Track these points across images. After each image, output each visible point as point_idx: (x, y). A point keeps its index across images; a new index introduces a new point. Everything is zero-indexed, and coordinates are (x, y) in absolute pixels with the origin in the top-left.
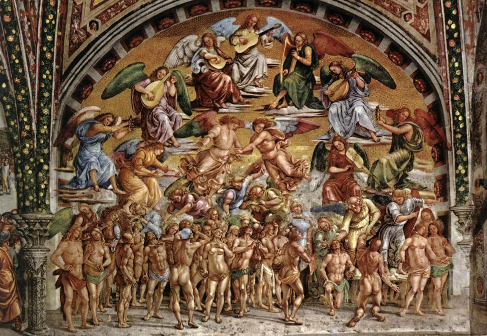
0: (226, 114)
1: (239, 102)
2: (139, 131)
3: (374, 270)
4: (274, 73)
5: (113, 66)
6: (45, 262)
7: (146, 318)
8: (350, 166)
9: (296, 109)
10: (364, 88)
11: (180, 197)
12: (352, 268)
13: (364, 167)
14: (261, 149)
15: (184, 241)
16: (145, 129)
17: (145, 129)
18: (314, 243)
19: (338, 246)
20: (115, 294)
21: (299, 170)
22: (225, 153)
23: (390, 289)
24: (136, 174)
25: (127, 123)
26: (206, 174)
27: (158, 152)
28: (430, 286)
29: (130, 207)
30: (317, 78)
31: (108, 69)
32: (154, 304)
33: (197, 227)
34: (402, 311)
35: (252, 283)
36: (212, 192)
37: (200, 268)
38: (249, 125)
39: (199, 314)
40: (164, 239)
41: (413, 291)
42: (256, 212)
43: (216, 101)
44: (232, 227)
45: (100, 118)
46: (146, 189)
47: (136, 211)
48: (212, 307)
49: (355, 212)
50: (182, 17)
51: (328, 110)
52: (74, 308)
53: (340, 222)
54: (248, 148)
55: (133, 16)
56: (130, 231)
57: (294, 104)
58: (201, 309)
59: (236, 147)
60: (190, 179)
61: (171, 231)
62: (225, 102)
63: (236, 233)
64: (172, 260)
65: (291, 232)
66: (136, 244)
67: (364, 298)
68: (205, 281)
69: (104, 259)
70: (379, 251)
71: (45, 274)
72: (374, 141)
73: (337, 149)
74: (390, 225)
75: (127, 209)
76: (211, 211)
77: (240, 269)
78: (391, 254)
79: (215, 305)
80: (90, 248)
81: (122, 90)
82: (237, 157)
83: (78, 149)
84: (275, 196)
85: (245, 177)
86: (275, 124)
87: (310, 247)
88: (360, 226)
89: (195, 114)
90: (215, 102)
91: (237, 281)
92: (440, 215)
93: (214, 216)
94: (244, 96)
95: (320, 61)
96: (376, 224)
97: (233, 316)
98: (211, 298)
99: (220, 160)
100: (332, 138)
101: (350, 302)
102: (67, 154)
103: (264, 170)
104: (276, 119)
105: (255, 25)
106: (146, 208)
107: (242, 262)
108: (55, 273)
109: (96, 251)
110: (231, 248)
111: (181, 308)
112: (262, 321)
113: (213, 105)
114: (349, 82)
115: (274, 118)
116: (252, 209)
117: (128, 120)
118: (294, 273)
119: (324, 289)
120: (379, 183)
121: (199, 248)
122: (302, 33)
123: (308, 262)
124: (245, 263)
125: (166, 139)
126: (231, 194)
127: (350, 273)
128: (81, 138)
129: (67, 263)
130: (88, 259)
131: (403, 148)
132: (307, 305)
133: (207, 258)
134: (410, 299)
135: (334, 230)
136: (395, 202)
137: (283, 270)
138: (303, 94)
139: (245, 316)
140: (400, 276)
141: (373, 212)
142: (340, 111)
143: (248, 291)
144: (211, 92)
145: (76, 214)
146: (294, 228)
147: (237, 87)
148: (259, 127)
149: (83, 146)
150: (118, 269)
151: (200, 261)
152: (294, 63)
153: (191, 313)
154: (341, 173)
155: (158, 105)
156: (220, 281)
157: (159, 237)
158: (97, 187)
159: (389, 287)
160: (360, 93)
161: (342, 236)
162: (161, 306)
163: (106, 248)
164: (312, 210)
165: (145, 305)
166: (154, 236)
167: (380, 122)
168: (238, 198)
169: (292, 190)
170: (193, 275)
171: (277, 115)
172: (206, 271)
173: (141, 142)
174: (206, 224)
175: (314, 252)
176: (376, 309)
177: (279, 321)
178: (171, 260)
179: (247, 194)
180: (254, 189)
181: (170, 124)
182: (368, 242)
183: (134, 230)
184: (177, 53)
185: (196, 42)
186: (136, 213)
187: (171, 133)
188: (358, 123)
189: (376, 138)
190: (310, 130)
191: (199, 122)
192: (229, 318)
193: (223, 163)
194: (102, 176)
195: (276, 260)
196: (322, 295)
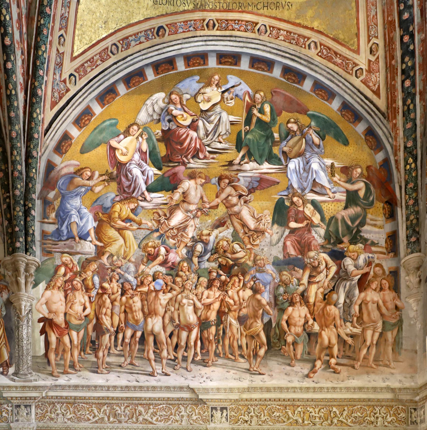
1: (205, 158)
2: (114, 185)
3: (331, 324)
4: (237, 129)
5: (90, 121)
6: (30, 310)
7: (123, 365)
8: (308, 221)
10: (319, 145)
11: (153, 250)
12: (311, 322)
13: (321, 223)
14: (227, 204)
15: (157, 291)
16: (120, 183)
17: (120, 183)
18: (276, 298)
19: (298, 300)
20: (95, 341)
22: (193, 207)
23: (345, 342)
24: (112, 226)
25: (104, 177)
27: (132, 206)
28: (382, 340)
29: (107, 258)
30: (276, 135)
31: (85, 125)
33: (169, 278)
34: (357, 364)
35: (219, 334)
36: (182, 245)
37: (172, 320)
38: (214, 180)
39: (172, 362)
40: (139, 290)
41: (366, 345)
42: (223, 265)
43: (184, 157)
44: (201, 279)
45: (79, 172)
46: (121, 241)
47: (113, 261)
48: (183, 356)
49: (313, 267)
50: (150, 75)
52: (57, 354)
53: (299, 276)
54: (214, 204)
55: (106, 72)
56: (108, 282)
57: (255, 161)
58: (173, 358)
59: (203, 202)
60: (162, 232)
61: (145, 281)
62: (193, 158)
63: (205, 285)
64: (146, 310)
66: (113, 294)
67: (322, 349)
68: (177, 331)
69: (85, 309)
70: (335, 305)
71: (30, 321)
72: (329, 197)
73: (296, 205)
74: (345, 279)
75: (105, 259)
78: (346, 309)
79: (186, 354)
80: (71, 298)
81: (98, 145)
82: (204, 211)
83: (59, 202)
86: (239, 180)
88: (317, 280)
89: (165, 169)
91: (206, 332)
92: (392, 270)
94: (210, 152)
95: (278, 118)
96: (333, 278)
97: (202, 365)
98: (182, 347)
99: (189, 214)
101: (309, 354)
102: (50, 206)
104: (239, 175)
105: (218, 83)
106: (122, 260)
107: (211, 314)
108: (40, 321)
109: (77, 300)
110: (200, 300)
111: (155, 357)
112: (229, 370)
114: (305, 138)
115: (237, 174)
117: (104, 175)
118: (258, 325)
119: (285, 341)
120: (335, 239)
121: (171, 299)
122: (261, 91)
123: (271, 315)
124: (213, 316)
125: (140, 193)
126: (199, 247)
127: (309, 326)
128: (62, 191)
129: (50, 312)
130: (70, 308)
131: (357, 205)
133: (178, 310)
134: (364, 351)
135: (294, 283)
136: (350, 257)
138: (264, 150)
139: (213, 365)
140: (355, 330)
141: (330, 266)
142: (297, 167)
143: (216, 341)
144: (179, 147)
145: (59, 264)
147: (203, 144)
149: (64, 198)
150: (98, 319)
151: (172, 312)
152: (254, 120)
153: (164, 361)
154: (300, 228)
155: (131, 160)
156: (190, 331)
157: (134, 287)
158: (77, 238)
159: (345, 340)
160: (316, 150)
161: (301, 288)
162: (137, 354)
163: (87, 298)
164: (274, 264)
165: (122, 353)
166: (130, 287)
167: (335, 179)
168: (206, 251)
169: (255, 243)
170: (166, 325)
172: (177, 322)
173: (117, 196)
174: (177, 275)
175: (276, 305)
176: (333, 361)
177: (244, 370)
179: (214, 248)
180: (221, 243)
182: (325, 295)
183: (111, 281)
184: (147, 110)
185: (164, 99)
186: (112, 264)
187: (144, 187)
188: (314, 180)
189: (331, 195)
190: (271, 186)
191: (169, 177)
192: (200, 367)
194: (82, 227)
195: (241, 312)
196: (284, 347)
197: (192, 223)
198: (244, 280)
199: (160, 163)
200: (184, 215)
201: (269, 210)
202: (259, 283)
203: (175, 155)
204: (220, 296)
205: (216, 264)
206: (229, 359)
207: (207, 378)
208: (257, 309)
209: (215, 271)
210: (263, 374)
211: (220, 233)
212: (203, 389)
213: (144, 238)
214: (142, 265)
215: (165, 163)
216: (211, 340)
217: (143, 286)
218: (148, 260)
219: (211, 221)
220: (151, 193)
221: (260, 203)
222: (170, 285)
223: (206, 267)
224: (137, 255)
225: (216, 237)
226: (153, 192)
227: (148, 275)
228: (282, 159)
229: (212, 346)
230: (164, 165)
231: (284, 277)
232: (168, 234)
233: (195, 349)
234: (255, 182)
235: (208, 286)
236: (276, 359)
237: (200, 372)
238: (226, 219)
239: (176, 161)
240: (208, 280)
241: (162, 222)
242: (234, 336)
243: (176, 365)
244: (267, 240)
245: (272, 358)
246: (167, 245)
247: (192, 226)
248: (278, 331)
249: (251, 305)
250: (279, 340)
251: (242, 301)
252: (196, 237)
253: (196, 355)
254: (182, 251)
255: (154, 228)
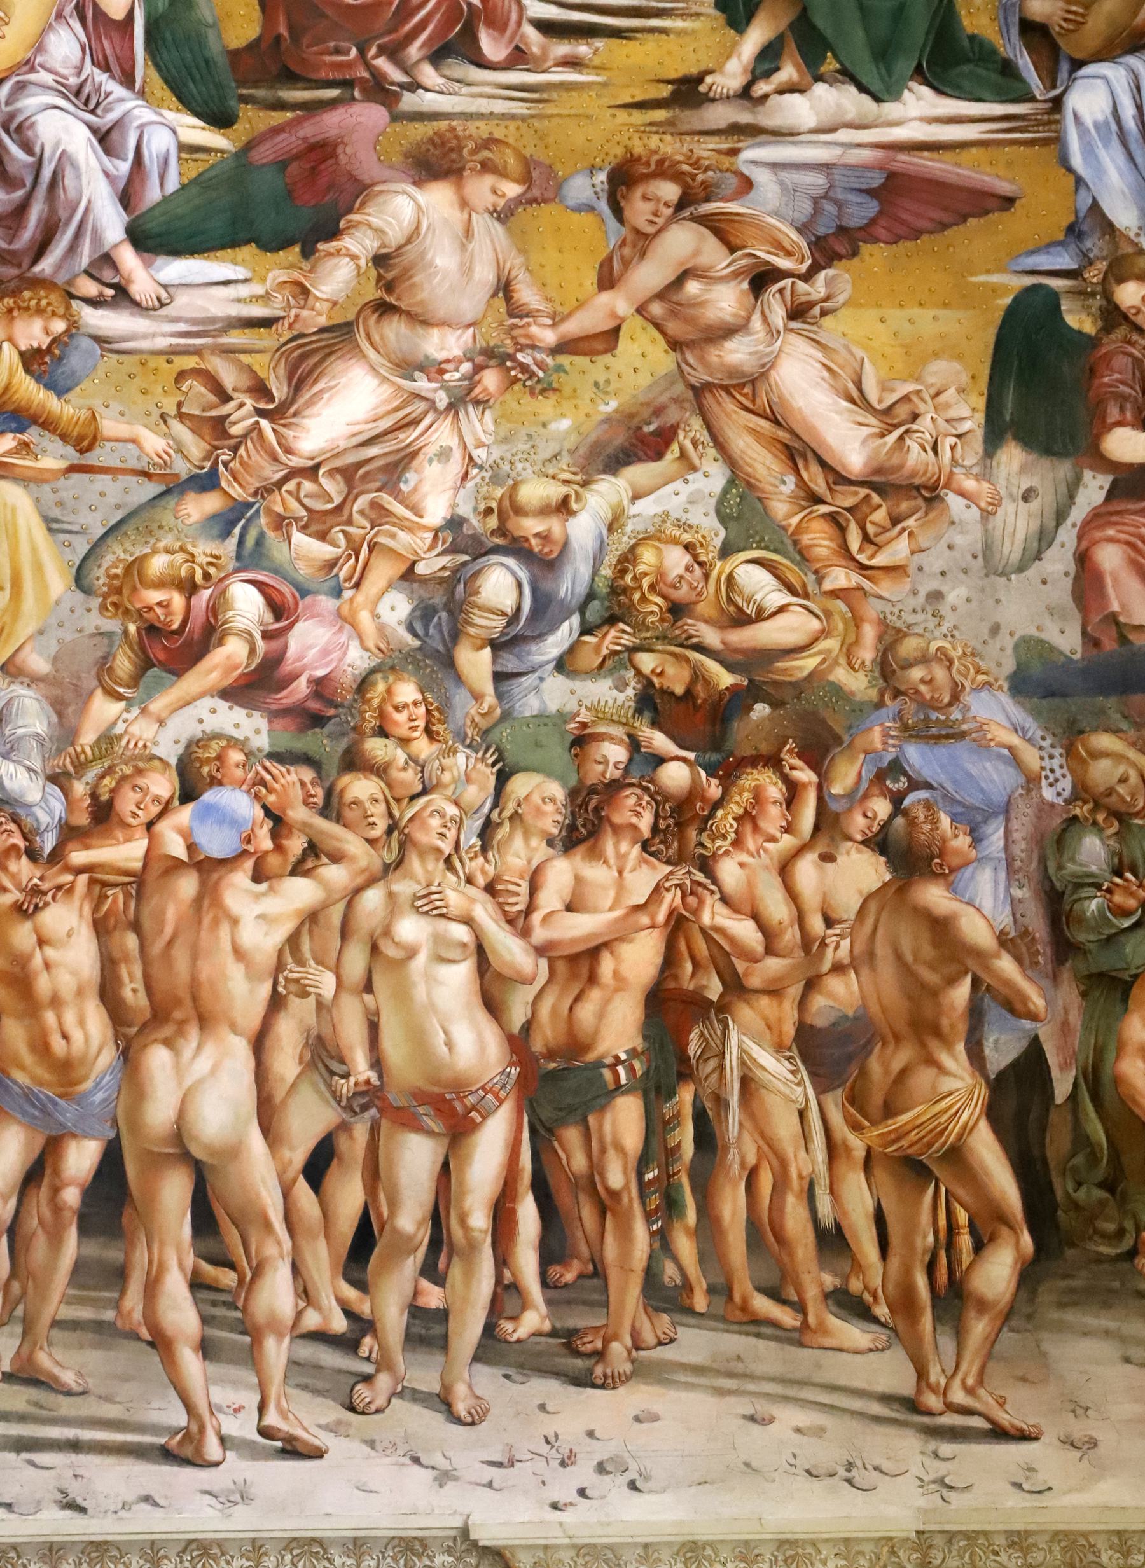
0: (443, 125)
1: (519, 57)
9: (865, 99)
11: (178, 601)
14: (673, 327)
21: (912, 444)
26: (338, 463)
32: (16, 1286)
33: (295, 777)
35: (672, 1153)
36: (383, 572)
39: (331, 1358)
40: (78, 857)
42: (667, 693)
43: (382, 51)
44: (520, 785)
48: (416, 1311)
51: (1057, 104)
57: (848, 75)
58: (339, 1324)
59: (515, 310)
60: (236, 492)
61: (127, 803)
62: (438, 56)
63: (551, 820)
64: (133, 993)
65: (899, 821)
68: (361, 1132)
76: (381, 687)
77: (591, 1057)
79: (433, 1297)
82: (524, 368)
84: (781, 597)
85: (585, 484)
86: (747, 184)
87: (1039, 926)
90: (373, 51)
91: (572, 1135)
93: (401, 717)
94: (547, 28)
97: (557, 1374)
98: (404, 1246)
99: (423, 384)
100: (1103, 265)
103: (695, 443)
104: (748, 154)
107: (601, 1015)
111: (205, 1320)
112: (763, 1408)
113: (364, 74)
115: (734, 152)
116: (638, 673)
118: (947, 1084)
121: (312, 917)
123: (1033, 1017)
125: (85, 257)
132: (1061, 1305)
133: (368, 987)
137: (875, 1065)
139: (642, 1372)
143: (654, 1201)
146: (922, 794)
148: (645, 198)
151: (320, 1005)
155: (29, 65)
157: (48, 843)
162: (66, 1300)
166: (18, 840)
169: (878, 561)
170: (279, 1095)
171: (753, 131)
172: (362, 1069)
174: (353, 762)
177: (876, 1408)
178: (127, 993)
179: (602, 587)
180: (648, 557)
181: (107, 175)
190: (964, 218)
191: (282, 165)
193: (442, 404)
197: (442, 434)
198: (820, 788)
199: (219, 86)
200: (386, 391)
201: (959, 357)
202: (928, 805)
203: (319, 40)
204: (657, 889)
205: (621, 686)
206: (755, 1324)
207: (601, 1468)
208: (931, 977)
209: (618, 731)
210: (1023, 1437)
211: (636, 497)
212: (578, 1549)
213: (113, 530)
214: (99, 696)
215: (256, 84)
216: (615, 1195)
217: (107, 835)
218: (145, 664)
219: (577, 428)
220: (161, 260)
221: (898, 318)
222: (305, 827)
223: (552, 707)
224: (69, 636)
225: (614, 525)
226: (176, 252)
227: (144, 761)
228: (1025, 64)
229: (625, 1235)
230: (244, 99)
231: (1102, 773)
232: (284, 502)
233: (502, 1260)
234: (853, 198)
235: (572, 828)
236: (1105, 1321)
237: (549, 1426)
238: (673, 415)
239: (323, 75)
240: (573, 794)
241: (236, 430)
242: (783, 1163)
243: (367, 1379)
244: (959, 540)
245: (1070, 1316)
246: (276, 571)
247: (444, 454)
248: (1096, 1130)
249: (882, 950)
250: (1109, 1185)
251: (816, 924)
252: (475, 521)
253: (510, 1303)
254: (383, 609)
255: (182, 468)
